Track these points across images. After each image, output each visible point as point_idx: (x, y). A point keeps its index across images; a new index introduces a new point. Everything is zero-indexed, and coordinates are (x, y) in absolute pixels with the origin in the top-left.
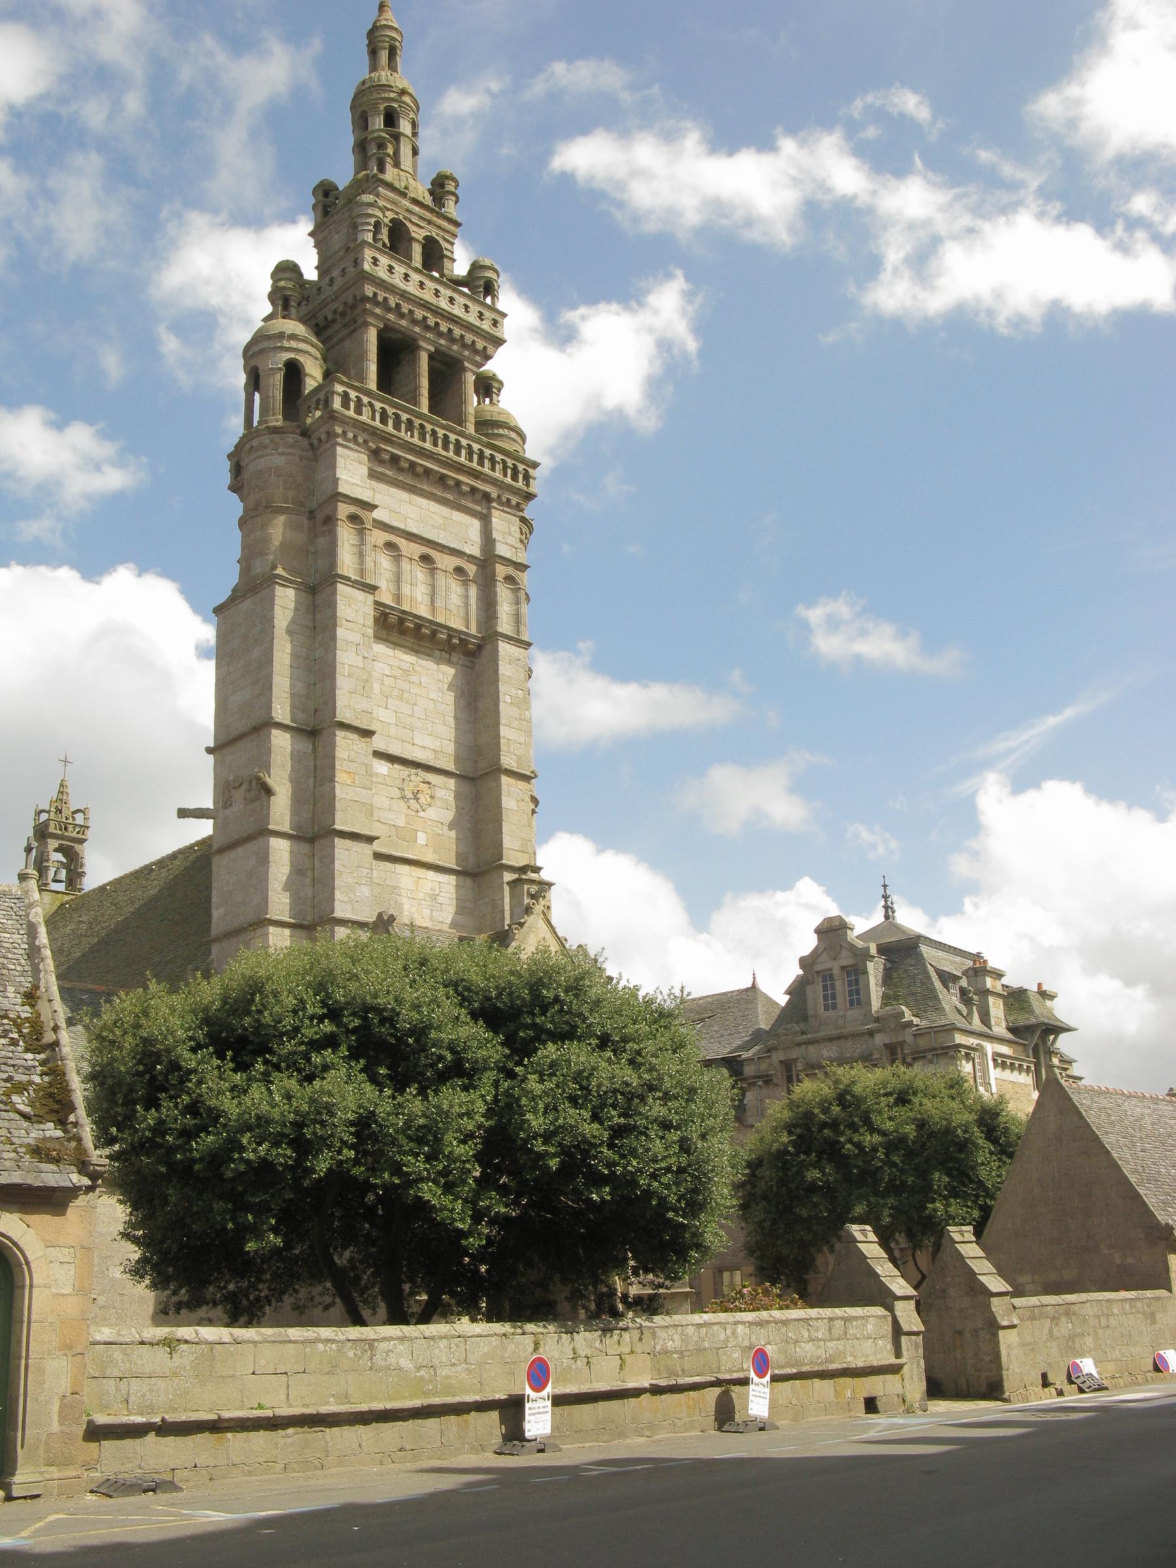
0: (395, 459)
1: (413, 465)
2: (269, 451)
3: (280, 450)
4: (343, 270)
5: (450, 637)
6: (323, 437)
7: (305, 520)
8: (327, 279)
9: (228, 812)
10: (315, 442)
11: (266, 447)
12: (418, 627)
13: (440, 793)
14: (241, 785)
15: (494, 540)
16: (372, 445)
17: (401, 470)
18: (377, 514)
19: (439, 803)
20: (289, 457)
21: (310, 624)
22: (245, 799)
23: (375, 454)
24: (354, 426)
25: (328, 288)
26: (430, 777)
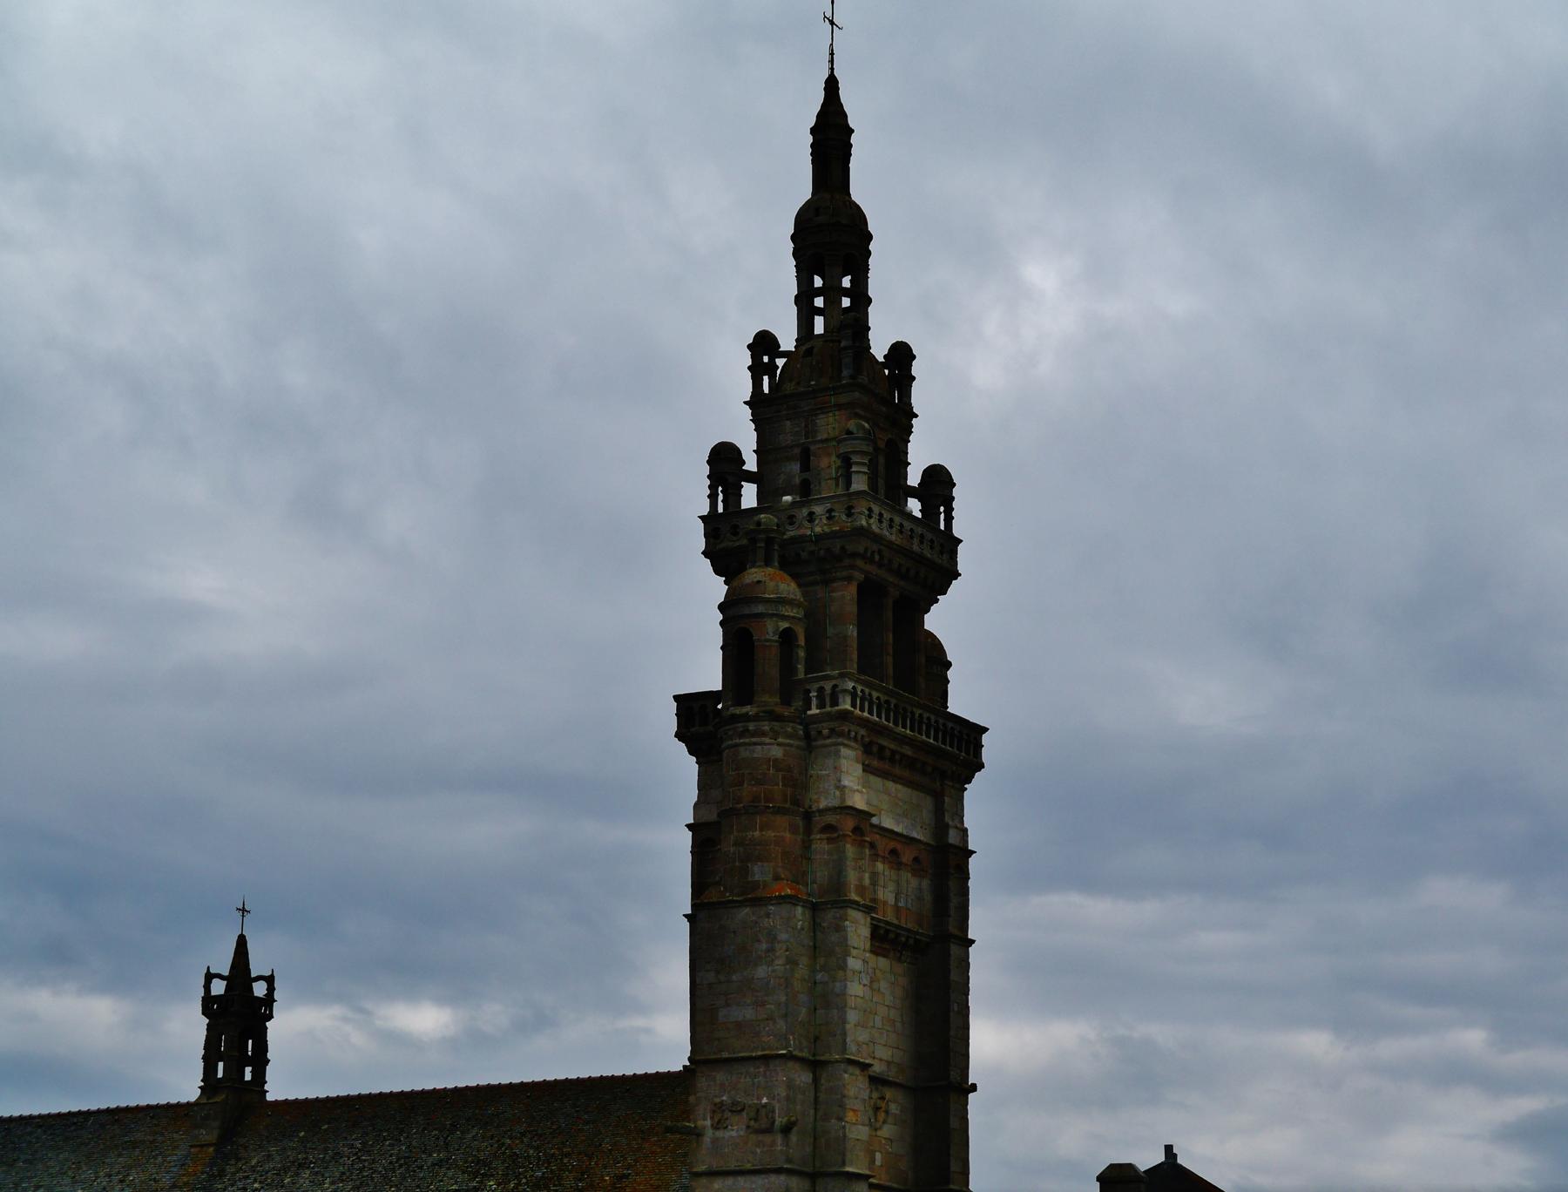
0: (882, 748)
1: (893, 752)
2: (767, 740)
3: (780, 740)
4: (830, 511)
5: (908, 938)
6: (826, 732)
7: (800, 823)
8: (805, 512)
9: (720, 1134)
10: (813, 733)
11: (764, 734)
12: (887, 931)
13: (894, 1108)
14: (743, 1110)
15: (947, 826)
16: (867, 740)
17: (881, 758)
18: (874, 820)
19: (890, 1119)
20: (787, 748)
21: (811, 944)
22: (748, 1127)
23: (867, 749)
24: (858, 725)
25: (806, 524)
26: (889, 1093)
